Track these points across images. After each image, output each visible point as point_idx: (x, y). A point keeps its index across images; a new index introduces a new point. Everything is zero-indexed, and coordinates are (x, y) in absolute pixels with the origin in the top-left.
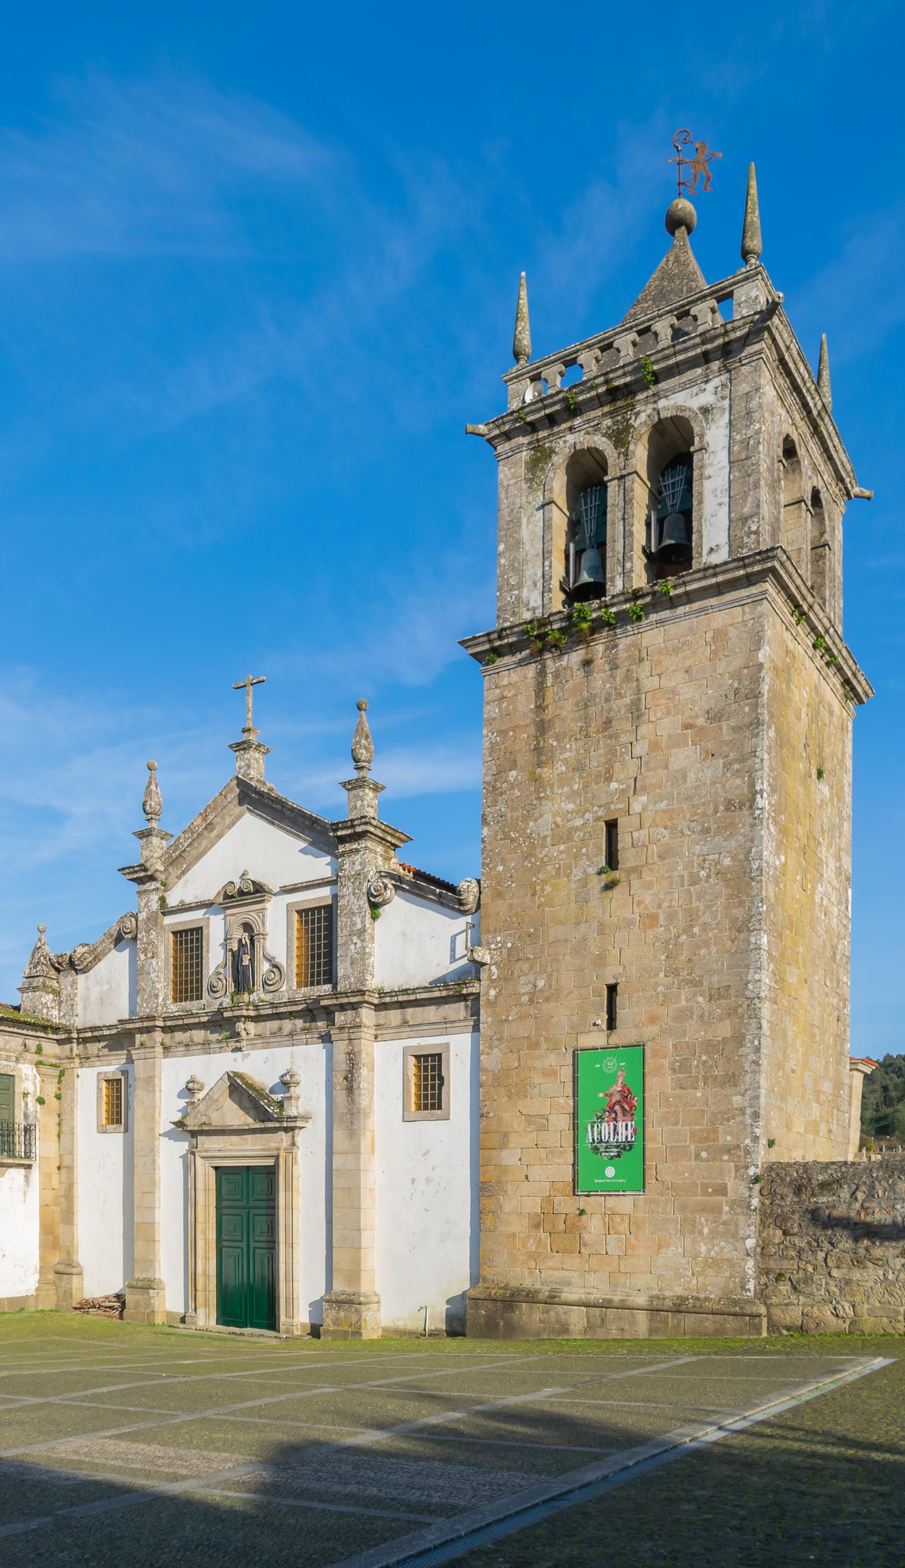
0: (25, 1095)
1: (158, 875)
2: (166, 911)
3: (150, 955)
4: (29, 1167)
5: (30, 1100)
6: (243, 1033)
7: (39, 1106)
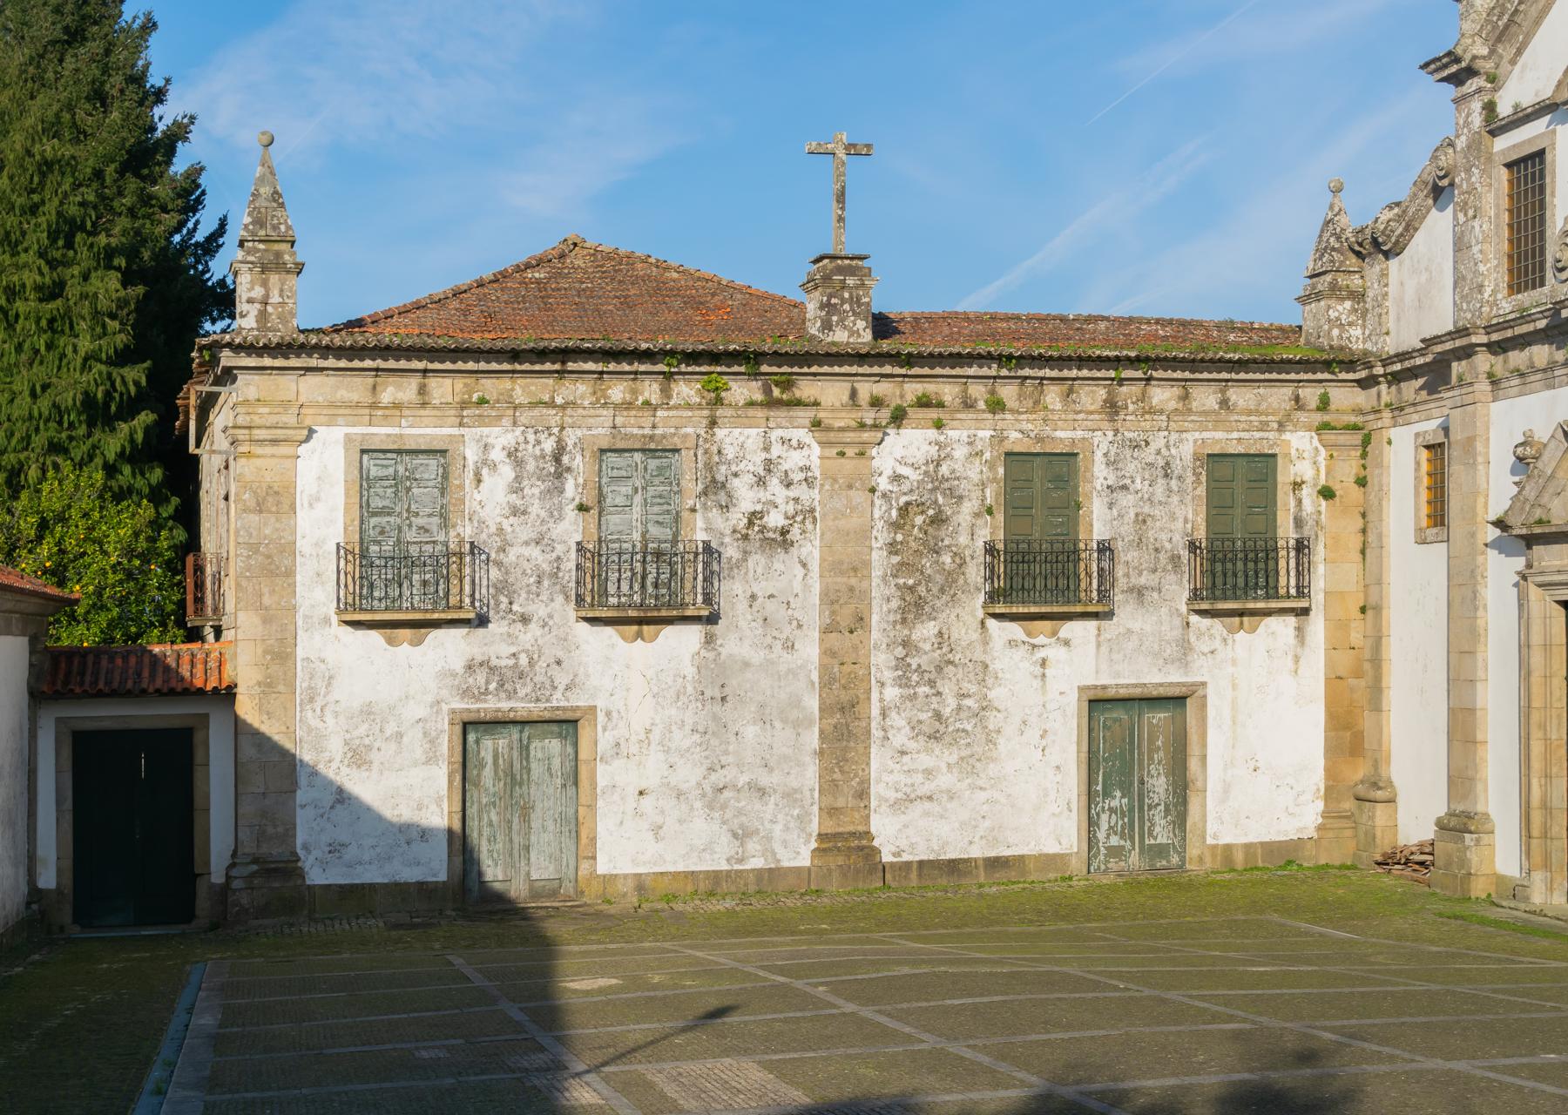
0: (1297, 485)
1: (1479, 64)
2: (1496, 127)
3: (1471, 213)
4: (1305, 612)
5: (1307, 494)
7: (1324, 503)
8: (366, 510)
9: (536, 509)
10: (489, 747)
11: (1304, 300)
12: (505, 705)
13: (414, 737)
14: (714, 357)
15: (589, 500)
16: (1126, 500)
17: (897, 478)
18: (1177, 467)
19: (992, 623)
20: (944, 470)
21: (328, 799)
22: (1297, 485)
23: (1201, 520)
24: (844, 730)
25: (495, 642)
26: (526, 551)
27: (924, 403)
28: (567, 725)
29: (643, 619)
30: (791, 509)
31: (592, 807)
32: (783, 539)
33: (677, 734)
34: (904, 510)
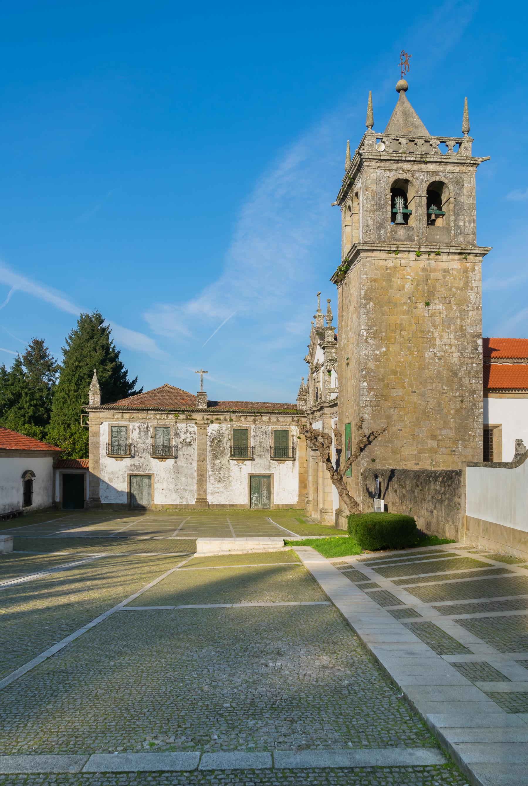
0: (293, 436)
8: (112, 437)
9: (143, 437)
10: (135, 480)
11: (297, 400)
12: (137, 472)
13: (121, 477)
14: (176, 411)
15: (153, 436)
16: (257, 438)
17: (212, 433)
18: (268, 432)
19: (230, 461)
20: (221, 432)
21: (105, 488)
22: (293, 436)
23: (273, 442)
24: (201, 479)
25: (136, 461)
26: (141, 445)
27: (217, 419)
28: (149, 477)
29: (163, 458)
30: (191, 438)
31: (154, 492)
32: (190, 444)
33: (169, 479)
34: (213, 439)
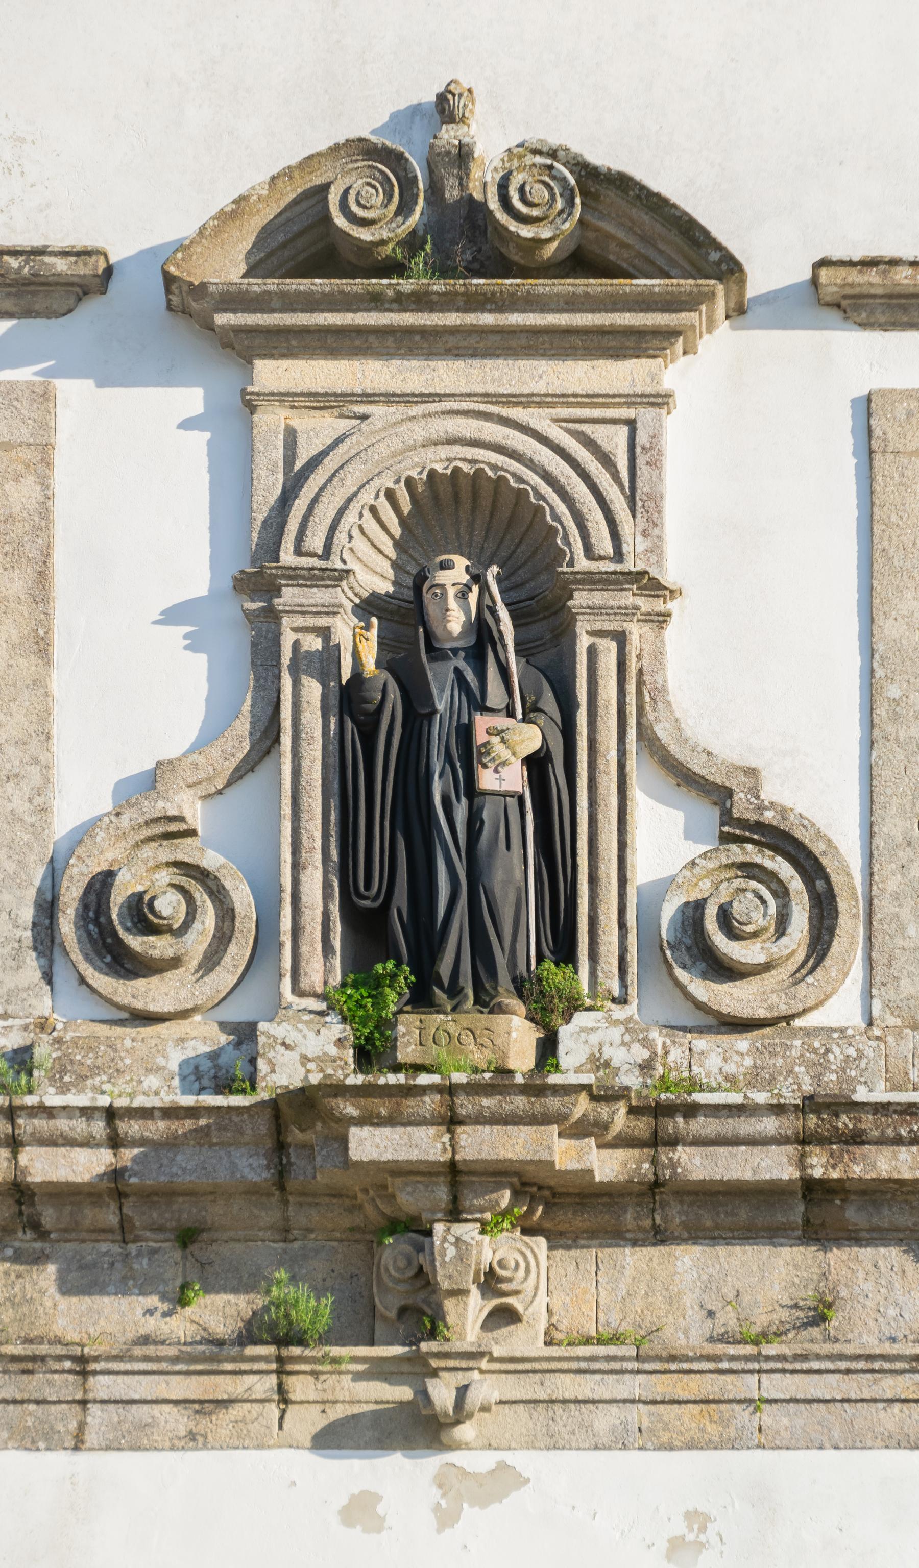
6: (468, 1316)
